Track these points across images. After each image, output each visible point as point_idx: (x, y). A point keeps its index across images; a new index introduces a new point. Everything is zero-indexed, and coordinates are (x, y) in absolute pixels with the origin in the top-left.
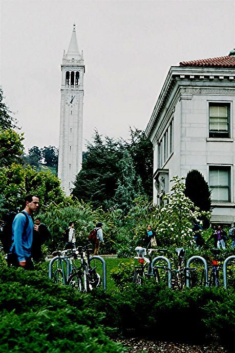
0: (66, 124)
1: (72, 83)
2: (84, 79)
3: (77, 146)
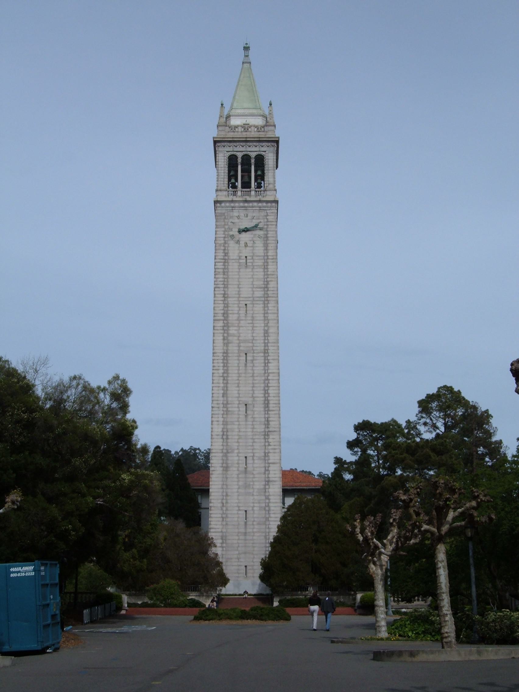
0: (232, 291)
1: (246, 185)
2: (283, 179)
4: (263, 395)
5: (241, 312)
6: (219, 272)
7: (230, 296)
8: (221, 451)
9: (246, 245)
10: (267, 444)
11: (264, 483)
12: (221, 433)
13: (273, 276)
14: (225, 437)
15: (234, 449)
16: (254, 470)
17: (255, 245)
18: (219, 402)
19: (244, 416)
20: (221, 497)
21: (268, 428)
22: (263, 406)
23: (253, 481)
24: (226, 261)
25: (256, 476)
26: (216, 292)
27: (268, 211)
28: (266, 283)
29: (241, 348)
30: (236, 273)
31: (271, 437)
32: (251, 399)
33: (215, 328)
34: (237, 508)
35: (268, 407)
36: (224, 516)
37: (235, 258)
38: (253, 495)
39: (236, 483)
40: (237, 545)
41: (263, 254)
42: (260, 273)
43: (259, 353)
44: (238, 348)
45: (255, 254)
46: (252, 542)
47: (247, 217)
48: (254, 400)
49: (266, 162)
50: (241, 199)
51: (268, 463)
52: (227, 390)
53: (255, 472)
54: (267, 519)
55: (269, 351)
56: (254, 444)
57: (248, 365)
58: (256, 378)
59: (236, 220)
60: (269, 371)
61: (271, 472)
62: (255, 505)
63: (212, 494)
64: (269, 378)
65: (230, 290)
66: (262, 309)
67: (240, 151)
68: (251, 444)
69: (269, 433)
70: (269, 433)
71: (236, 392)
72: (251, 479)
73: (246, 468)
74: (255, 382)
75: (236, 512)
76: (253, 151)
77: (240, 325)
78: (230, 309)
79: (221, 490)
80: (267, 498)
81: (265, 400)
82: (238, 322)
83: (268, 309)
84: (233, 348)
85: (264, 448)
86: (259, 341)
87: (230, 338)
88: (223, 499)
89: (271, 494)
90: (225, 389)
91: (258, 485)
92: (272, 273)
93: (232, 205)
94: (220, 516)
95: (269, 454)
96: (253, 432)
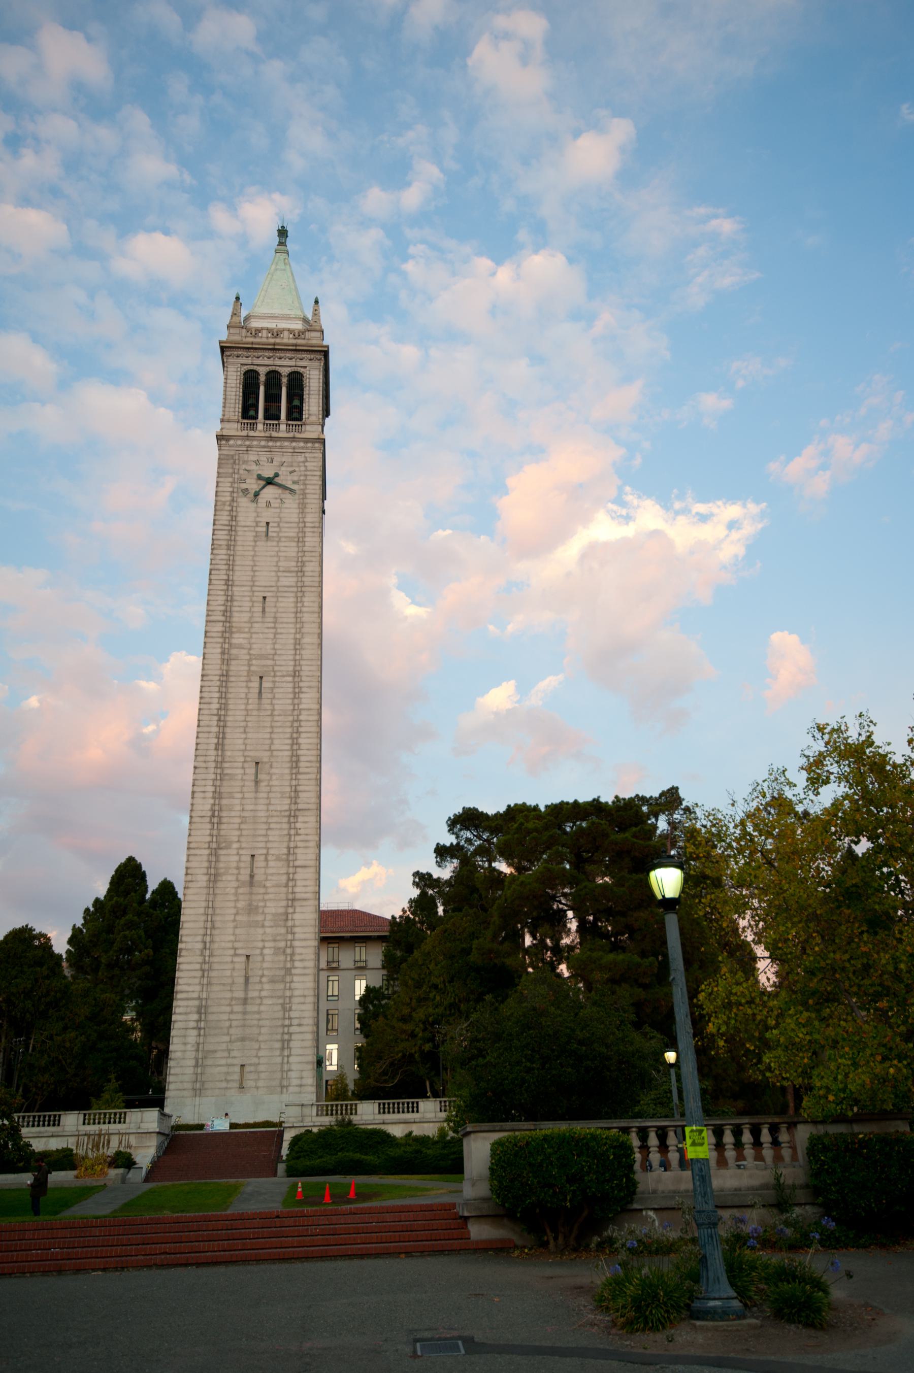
0: (241, 576)
3: (296, 674)
4: (288, 747)
5: (255, 609)
6: (220, 545)
7: (236, 583)
8: (206, 846)
9: (268, 504)
10: (292, 832)
11: (284, 903)
12: (209, 814)
13: (313, 554)
14: (215, 820)
15: (231, 842)
16: (267, 880)
17: (284, 506)
18: (208, 759)
19: (253, 784)
20: (202, 932)
21: (296, 803)
22: (289, 765)
23: (264, 900)
24: (232, 528)
25: (270, 890)
26: (213, 577)
27: (307, 455)
28: (299, 564)
29: (253, 668)
30: (251, 548)
31: (300, 819)
32: (268, 753)
33: (208, 634)
34: (232, 952)
36: (206, 967)
37: (248, 524)
38: (263, 926)
39: (232, 904)
40: (227, 1024)
42: (291, 550)
43: (284, 676)
44: (246, 668)
45: (284, 520)
46: (257, 1016)
47: (272, 462)
48: (272, 756)
49: (306, 382)
50: (263, 434)
51: (296, 867)
52: (224, 738)
53: (268, 884)
54: (288, 972)
55: (302, 673)
56: (269, 832)
57: (264, 696)
58: (277, 718)
59: (253, 467)
60: (301, 707)
61: (299, 883)
62: (267, 944)
63: (185, 925)
64: (301, 718)
65: (237, 573)
66: (293, 605)
67: (263, 365)
68: (264, 832)
69: (297, 813)
70: (297, 813)
71: (241, 741)
72: (260, 897)
73: (252, 876)
74: (275, 724)
75: (229, 959)
76: (285, 366)
77: (253, 630)
78: (235, 603)
79: (203, 918)
81: (292, 756)
82: (249, 625)
83: (303, 606)
84: (238, 668)
85: (286, 839)
86: (285, 657)
88: (205, 935)
89: (297, 923)
90: (221, 736)
91: (274, 907)
92: (310, 549)
93: (247, 443)
94: (198, 966)
95: (297, 851)
96: (268, 810)
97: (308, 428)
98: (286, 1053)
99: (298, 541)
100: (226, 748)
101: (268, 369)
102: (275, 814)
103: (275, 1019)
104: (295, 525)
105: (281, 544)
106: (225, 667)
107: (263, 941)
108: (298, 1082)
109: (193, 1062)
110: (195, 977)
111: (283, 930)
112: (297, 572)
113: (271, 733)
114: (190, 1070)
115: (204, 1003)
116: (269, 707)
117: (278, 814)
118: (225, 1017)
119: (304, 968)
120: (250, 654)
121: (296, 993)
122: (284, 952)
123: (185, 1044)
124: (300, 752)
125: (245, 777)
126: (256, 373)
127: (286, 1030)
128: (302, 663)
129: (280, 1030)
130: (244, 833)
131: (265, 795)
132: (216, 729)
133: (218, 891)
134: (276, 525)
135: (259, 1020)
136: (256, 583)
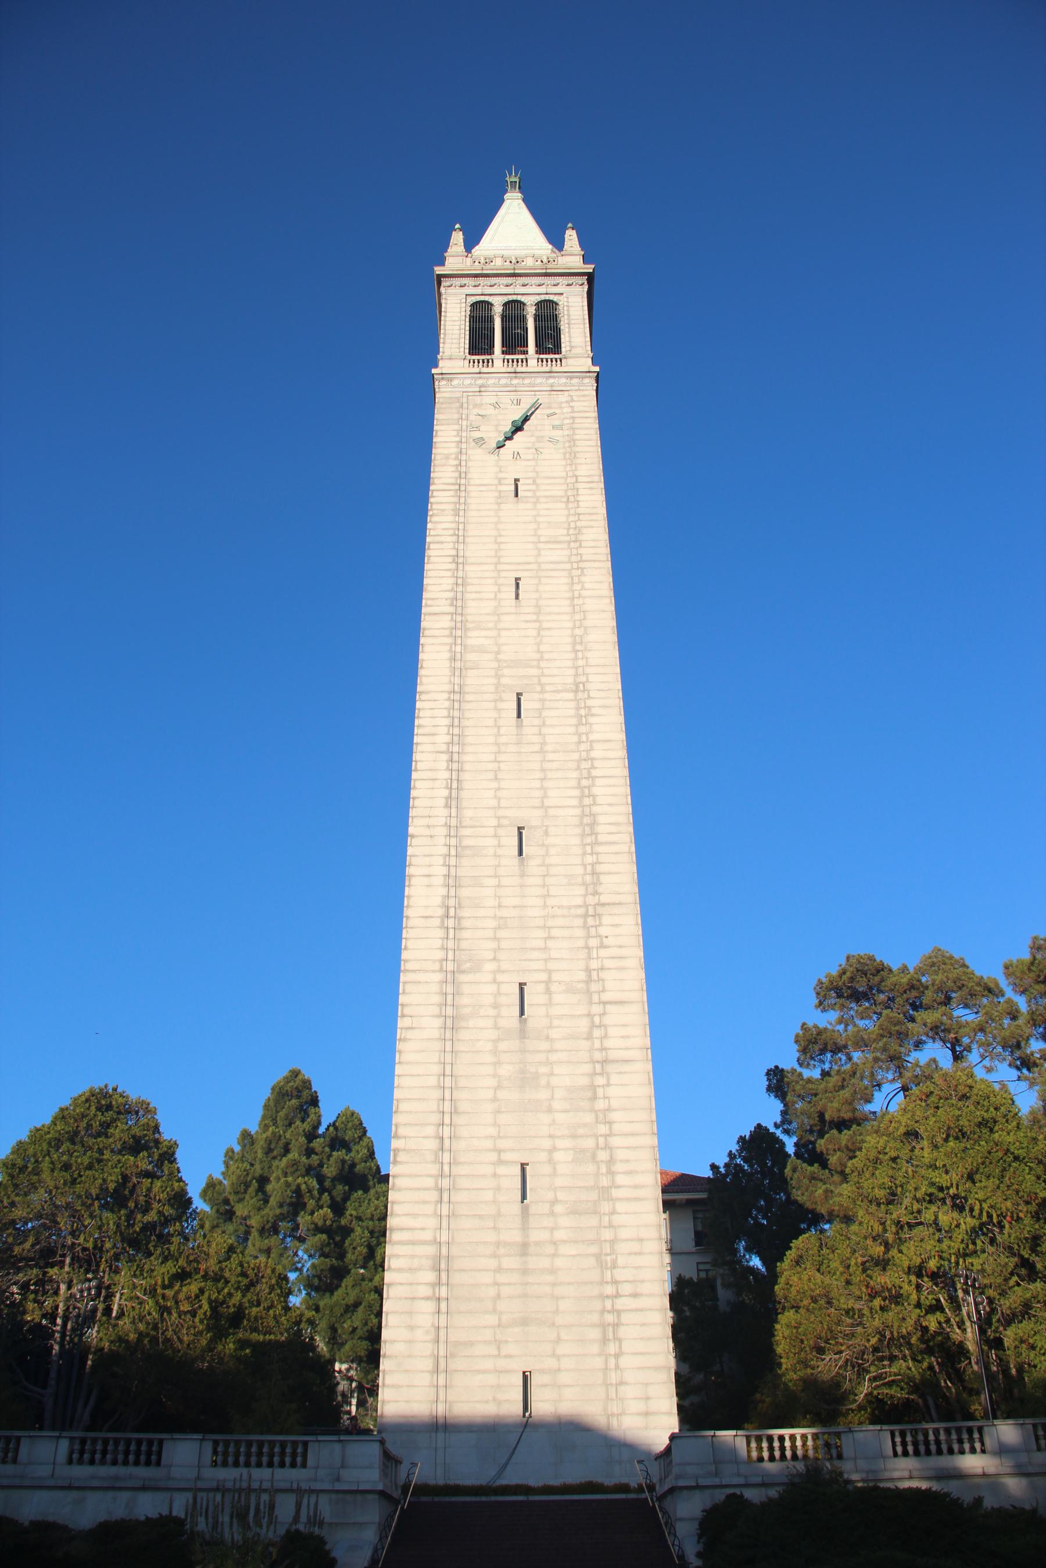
3: (579, 688)
4: (575, 802)
6: (443, 510)
7: (470, 560)
8: (437, 966)
9: (517, 456)
11: (587, 1068)
12: (440, 912)
13: (594, 517)
16: (551, 1027)
18: (432, 821)
20: (435, 1118)
21: (595, 893)
22: (578, 830)
23: (548, 1063)
27: (571, 393)
29: (504, 681)
31: (606, 920)
32: (539, 813)
34: (493, 1157)
35: (593, 833)
36: (445, 1183)
38: (550, 1110)
40: (492, 1292)
41: (564, 474)
43: (558, 691)
44: (493, 681)
46: (550, 1278)
51: (605, 1003)
53: (554, 1034)
54: (605, 1193)
55: (588, 686)
56: (550, 944)
58: (550, 756)
59: (491, 411)
61: (612, 1031)
62: (560, 1143)
63: (403, 1106)
68: (540, 944)
69: (600, 910)
70: (600, 910)
72: (542, 1057)
74: (546, 765)
75: (489, 1170)
78: (469, 588)
79: (437, 1094)
80: (603, 1117)
81: (583, 815)
82: (496, 618)
85: (583, 954)
87: (470, 657)
89: (614, 1103)
90: (455, 785)
94: (430, 1182)
96: (545, 906)
97: (570, 361)
98: (612, 1348)
99: (568, 501)
100: (465, 804)
101: (506, 299)
102: (560, 912)
103: (586, 1283)
104: (562, 481)
105: (539, 506)
106: (457, 680)
107: (551, 1136)
108: (640, 1406)
109: (429, 1364)
110: (425, 1202)
111: (589, 1118)
112: (569, 542)
113: (542, 780)
114: (426, 1379)
115: (444, 1251)
116: (536, 739)
117: (565, 912)
118: (487, 1278)
119: (636, 1187)
120: (498, 661)
121: (623, 1234)
122: (594, 1156)
123: (411, 1328)
124: (596, 809)
125: (500, 852)
126: (489, 305)
127: (608, 1304)
128: (588, 670)
129: (597, 1305)
130: (504, 944)
131: (539, 881)
132: (447, 775)
133: (460, 1047)
134: (530, 481)
135: (554, 1285)
136: (502, 560)
